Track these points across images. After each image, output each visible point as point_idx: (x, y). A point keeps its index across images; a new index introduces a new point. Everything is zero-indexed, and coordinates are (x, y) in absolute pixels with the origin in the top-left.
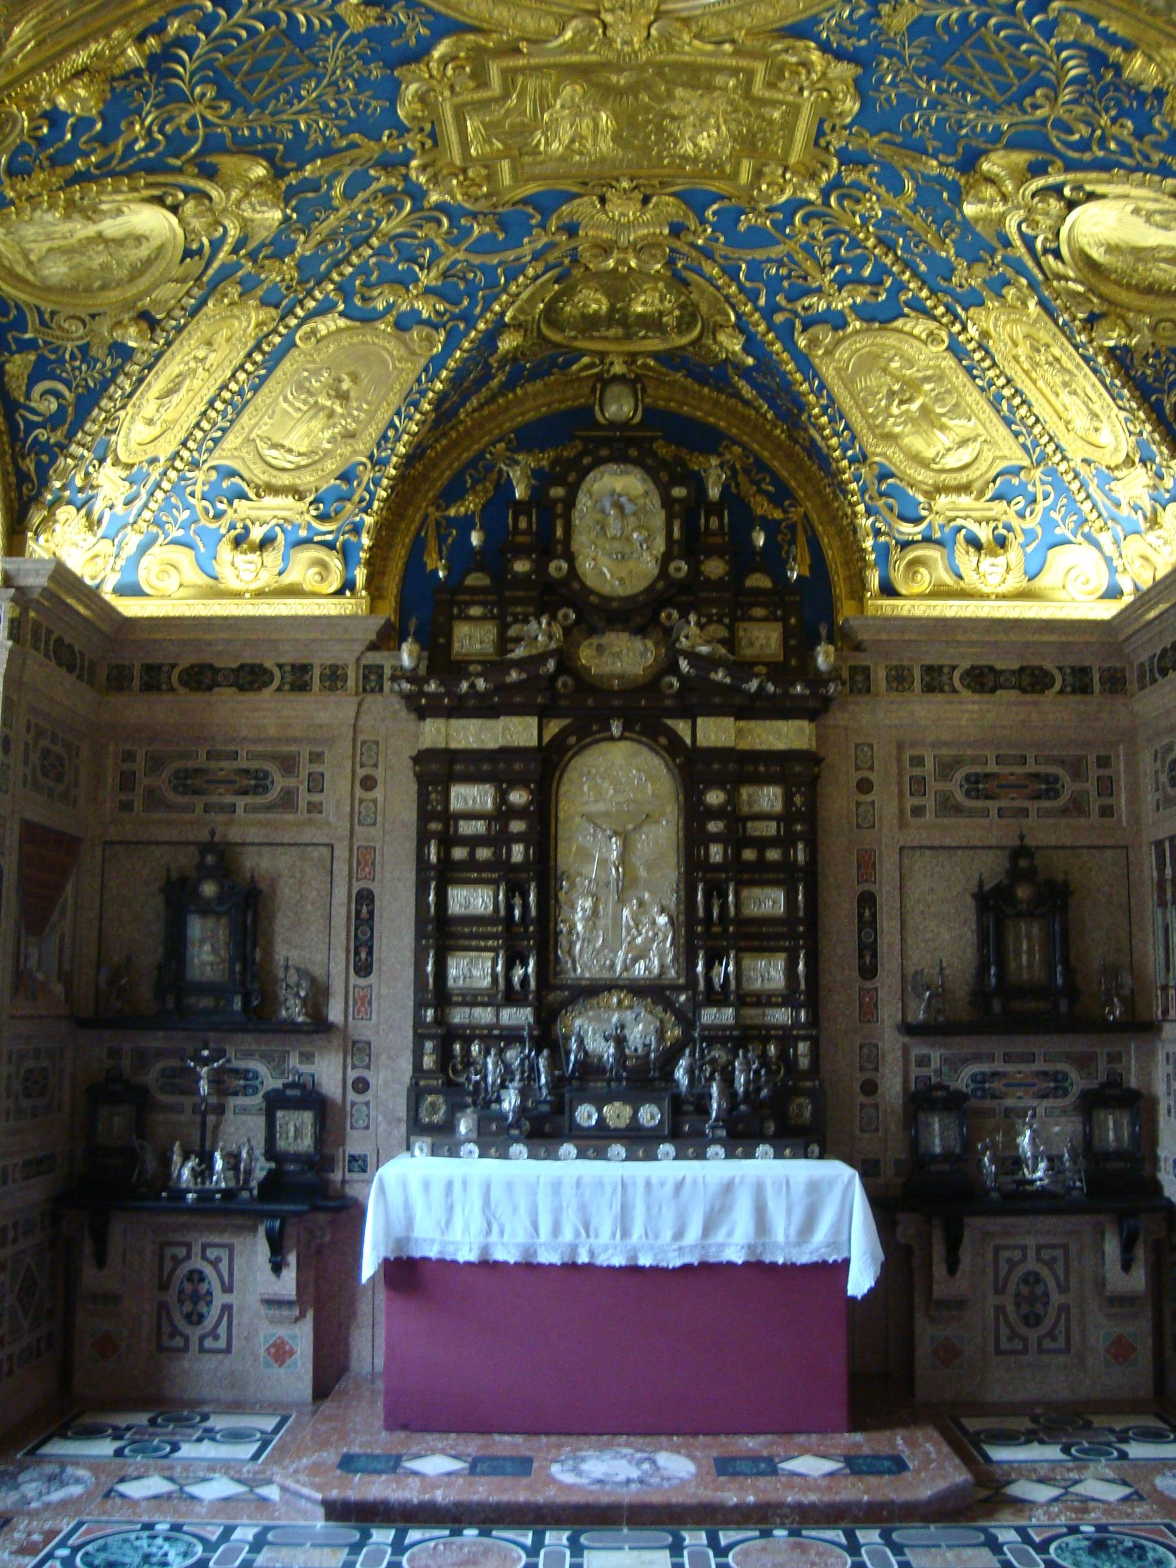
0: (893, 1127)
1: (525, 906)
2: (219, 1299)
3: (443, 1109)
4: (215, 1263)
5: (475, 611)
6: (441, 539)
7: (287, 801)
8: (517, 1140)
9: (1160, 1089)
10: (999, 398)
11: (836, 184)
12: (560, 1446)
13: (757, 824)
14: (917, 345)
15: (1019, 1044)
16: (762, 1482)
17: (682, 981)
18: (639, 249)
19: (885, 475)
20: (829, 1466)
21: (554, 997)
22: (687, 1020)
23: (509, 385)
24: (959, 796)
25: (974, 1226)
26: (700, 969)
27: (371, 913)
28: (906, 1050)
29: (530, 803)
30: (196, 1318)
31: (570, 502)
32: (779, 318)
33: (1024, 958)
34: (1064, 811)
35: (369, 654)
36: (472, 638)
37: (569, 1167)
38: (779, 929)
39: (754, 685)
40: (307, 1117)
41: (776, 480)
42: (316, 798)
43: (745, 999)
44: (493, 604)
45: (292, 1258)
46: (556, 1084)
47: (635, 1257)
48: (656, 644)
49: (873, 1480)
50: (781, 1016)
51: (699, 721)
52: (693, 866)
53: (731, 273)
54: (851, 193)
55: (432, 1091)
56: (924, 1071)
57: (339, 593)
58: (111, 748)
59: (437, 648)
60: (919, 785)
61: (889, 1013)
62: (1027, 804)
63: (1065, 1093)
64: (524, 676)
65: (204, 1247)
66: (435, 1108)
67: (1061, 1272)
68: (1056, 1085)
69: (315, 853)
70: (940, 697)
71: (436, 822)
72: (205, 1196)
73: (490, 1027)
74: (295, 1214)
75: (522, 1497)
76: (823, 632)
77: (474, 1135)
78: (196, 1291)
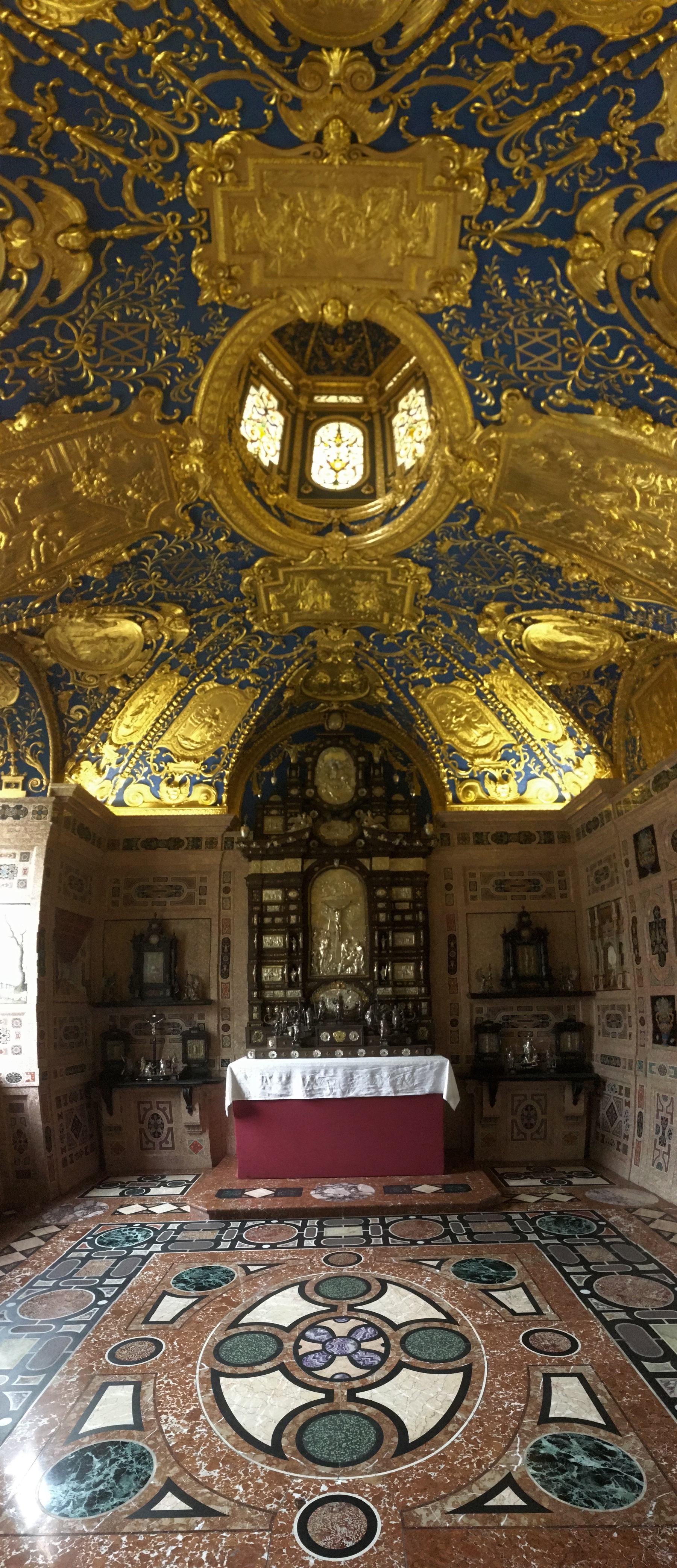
5: (274, 812)
6: (259, 781)
10: (501, 713)
11: (424, 623)
14: (463, 692)
15: (524, 1002)
18: (340, 653)
19: (451, 749)
21: (310, 984)
22: (371, 994)
23: (289, 716)
28: (471, 1006)
31: (315, 763)
32: (402, 682)
36: (273, 824)
39: (397, 842)
41: (404, 755)
43: (396, 984)
50: (413, 991)
52: (373, 924)
53: (381, 662)
54: (431, 627)
60: (473, 886)
61: (463, 989)
68: (543, 1021)
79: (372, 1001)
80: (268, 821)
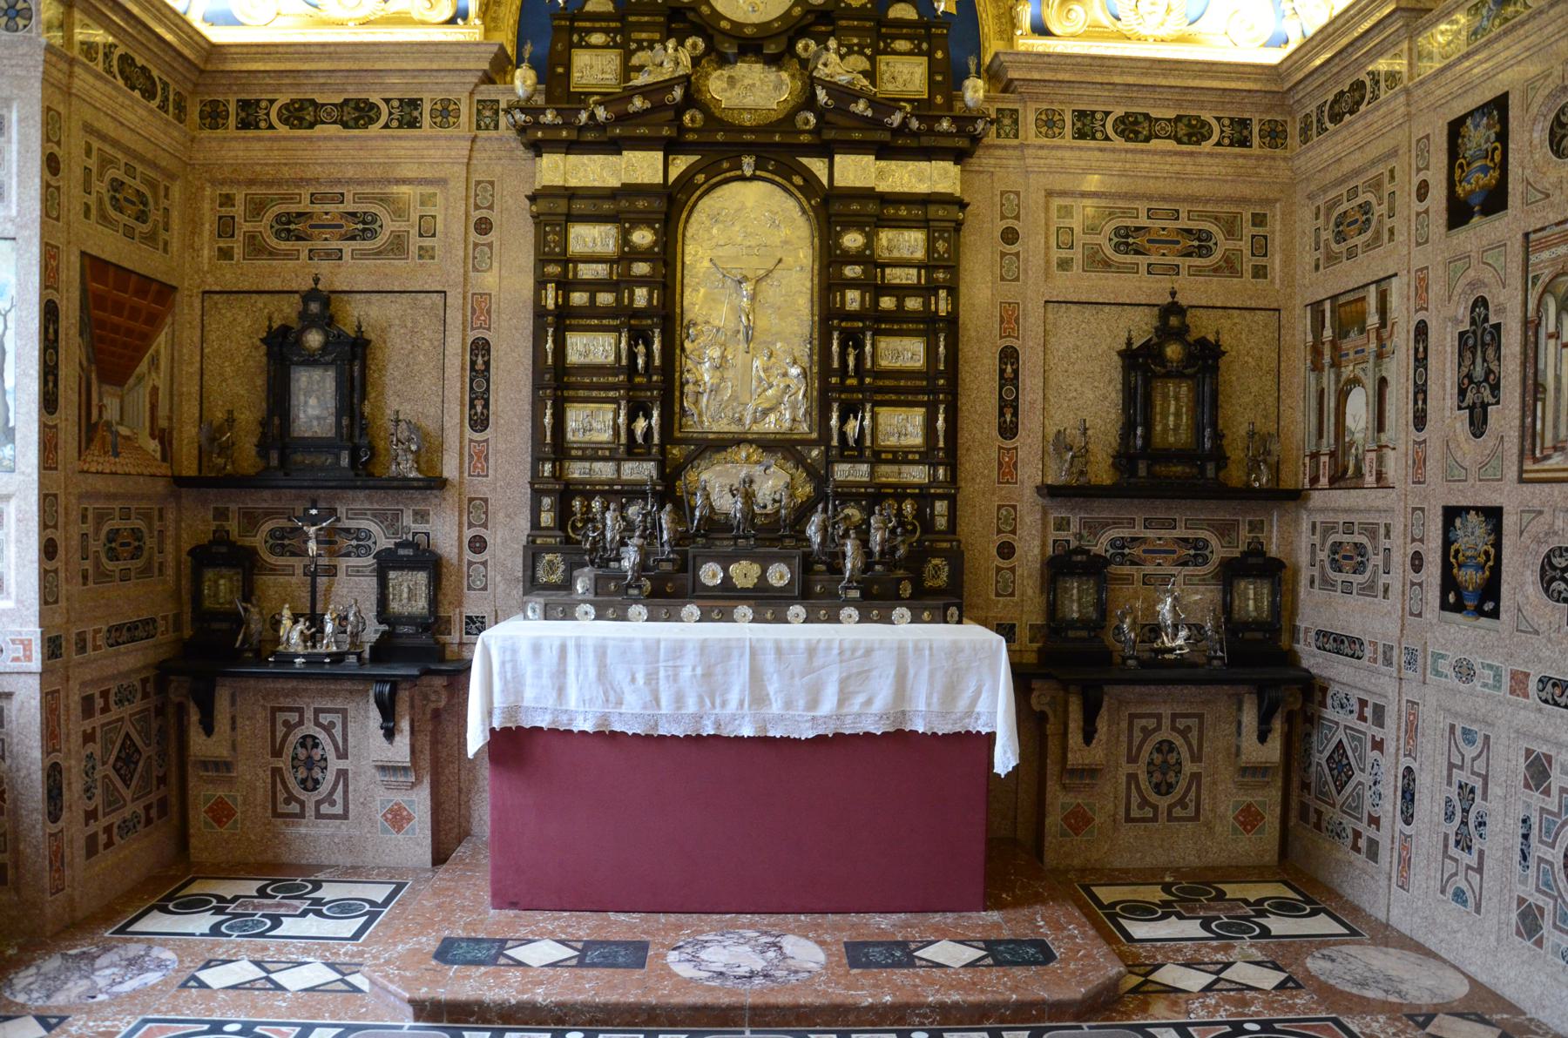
0: (1030, 592)
1: (649, 355)
2: (334, 764)
3: (562, 567)
4: (328, 729)
5: (597, 38)
7: (397, 246)
8: (636, 602)
9: (1304, 559)
12: (680, 927)
13: (898, 271)
16: (899, 975)
17: (814, 435)
20: (971, 954)
21: (676, 450)
22: (819, 476)
24: (1109, 251)
25: (1111, 694)
26: (834, 422)
27: (487, 364)
28: (1045, 513)
29: (655, 243)
30: (311, 784)
33: (1171, 418)
34: (1216, 270)
35: (483, 87)
36: (594, 68)
37: (690, 630)
38: (918, 383)
40: (422, 577)
42: (427, 242)
44: (616, 31)
45: (405, 725)
46: (680, 540)
47: (765, 729)
48: (793, 76)
49: (1019, 972)
50: (917, 474)
51: (837, 158)
52: (828, 316)
55: (550, 549)
56: (1062, 535)
57: (452, 21)
58: (208, 192)
59: (554, 75)
62: (1178, 261)
63: (1205, 562)
64: (648, 105)
65: (317, 711)
66: (552, 567)
67: (1195, 743)
68: (1196, 552)
69: (427, 300)
70: (1092, 143)
71: (554, 263)
72: (313, 660)
73: (611, 483)
74: (406, 678)
75: (632, 996)
76: (973, 68)
77: (591, 596)
78: (309, 757)
79: (825, 493)
80: (581, 59)
